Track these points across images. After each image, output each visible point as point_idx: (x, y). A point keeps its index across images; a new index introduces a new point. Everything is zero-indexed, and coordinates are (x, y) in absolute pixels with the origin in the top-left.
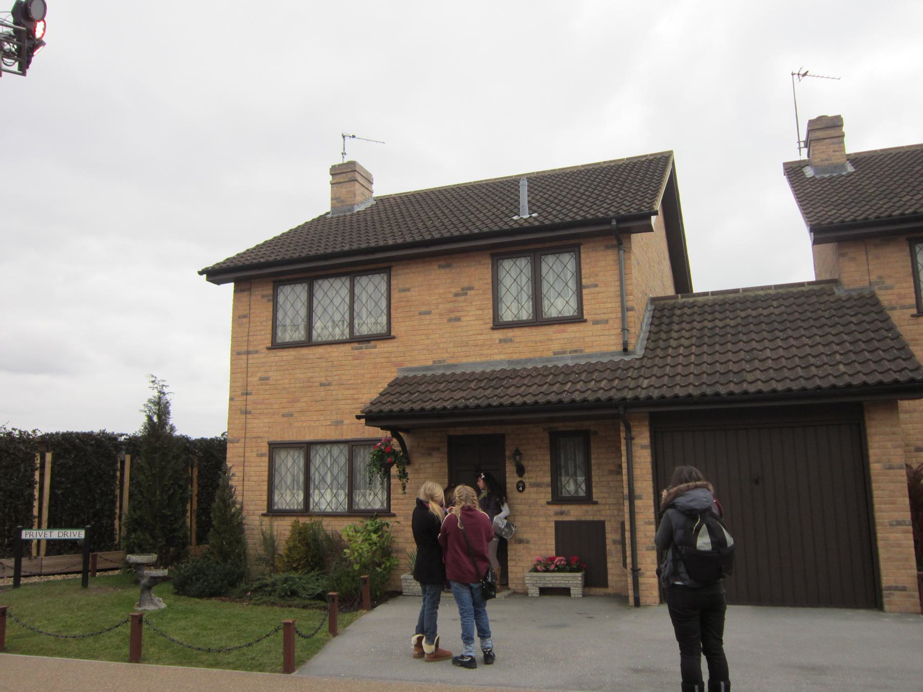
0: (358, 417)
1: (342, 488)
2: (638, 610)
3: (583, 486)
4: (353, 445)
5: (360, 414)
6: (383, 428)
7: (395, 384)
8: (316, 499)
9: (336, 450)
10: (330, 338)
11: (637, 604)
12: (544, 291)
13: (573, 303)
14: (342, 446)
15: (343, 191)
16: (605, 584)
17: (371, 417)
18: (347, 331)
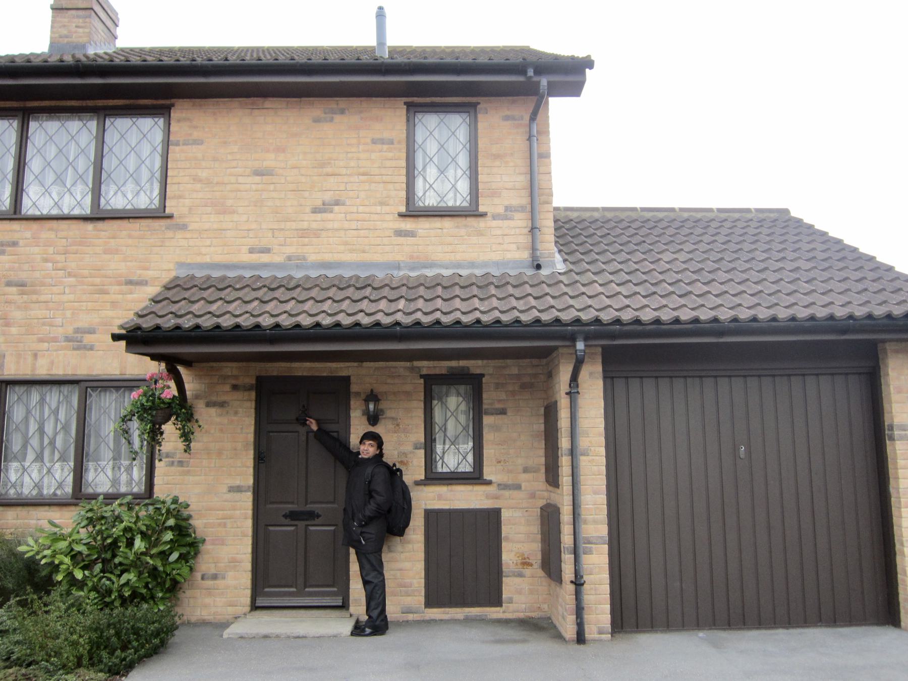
0: (116, 337)
1: (63, 458)
2: (582, 647)
3: (470, 458)
4: (87, 387)
5: (118, 331)
6: (154, 357)
7: (173, 286)
8: (13, 477)
9: (53, 397)
10: (55, 212)
11: (581, 639)
12: (419, 164)
13: (464, 186)
14: (65, 389)
15: (72, 21)
16: (496, 601)
17: (136, 338)
18: (88, 200)
